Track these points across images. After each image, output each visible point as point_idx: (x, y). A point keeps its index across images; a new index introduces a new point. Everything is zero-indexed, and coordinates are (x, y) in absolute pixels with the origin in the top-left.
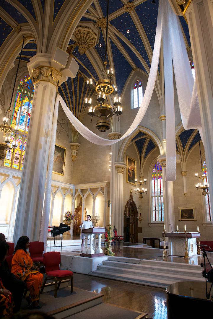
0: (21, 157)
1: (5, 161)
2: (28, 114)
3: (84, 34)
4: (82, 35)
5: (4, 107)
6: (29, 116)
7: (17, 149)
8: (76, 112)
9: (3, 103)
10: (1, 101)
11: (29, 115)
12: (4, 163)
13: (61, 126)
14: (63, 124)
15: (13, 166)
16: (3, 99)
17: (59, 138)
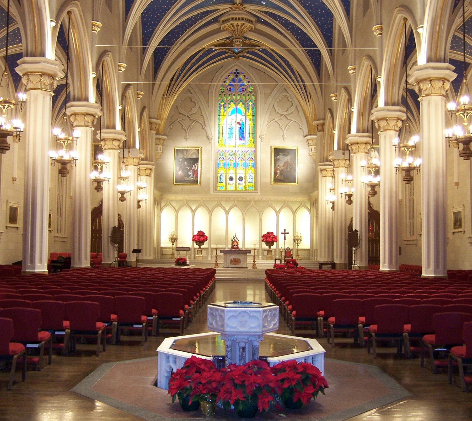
0: (236, 177)
1: (218, 186)
2: (237, 123)
3: (237, 26)
4: (236, 27)
5: (206, 129)
6: (238, 125)
7: (229, 168)
8: (302, 91)
9: (203, 125)
10: (201, 124)
11: (239, 123)
12: (218, 188)
13: (286, 119)
14: (288, 115)
15: (228, 188)
16: (203, 120)
17: (286, 136)
